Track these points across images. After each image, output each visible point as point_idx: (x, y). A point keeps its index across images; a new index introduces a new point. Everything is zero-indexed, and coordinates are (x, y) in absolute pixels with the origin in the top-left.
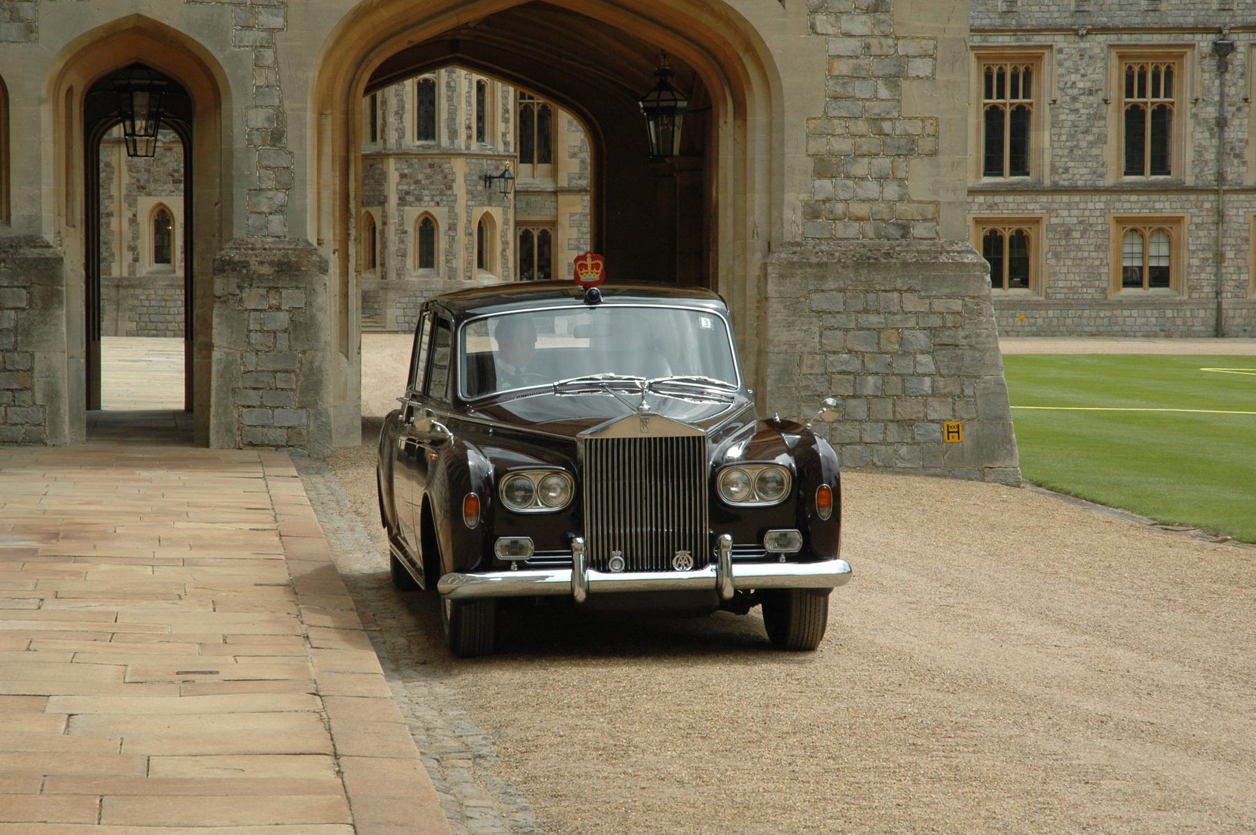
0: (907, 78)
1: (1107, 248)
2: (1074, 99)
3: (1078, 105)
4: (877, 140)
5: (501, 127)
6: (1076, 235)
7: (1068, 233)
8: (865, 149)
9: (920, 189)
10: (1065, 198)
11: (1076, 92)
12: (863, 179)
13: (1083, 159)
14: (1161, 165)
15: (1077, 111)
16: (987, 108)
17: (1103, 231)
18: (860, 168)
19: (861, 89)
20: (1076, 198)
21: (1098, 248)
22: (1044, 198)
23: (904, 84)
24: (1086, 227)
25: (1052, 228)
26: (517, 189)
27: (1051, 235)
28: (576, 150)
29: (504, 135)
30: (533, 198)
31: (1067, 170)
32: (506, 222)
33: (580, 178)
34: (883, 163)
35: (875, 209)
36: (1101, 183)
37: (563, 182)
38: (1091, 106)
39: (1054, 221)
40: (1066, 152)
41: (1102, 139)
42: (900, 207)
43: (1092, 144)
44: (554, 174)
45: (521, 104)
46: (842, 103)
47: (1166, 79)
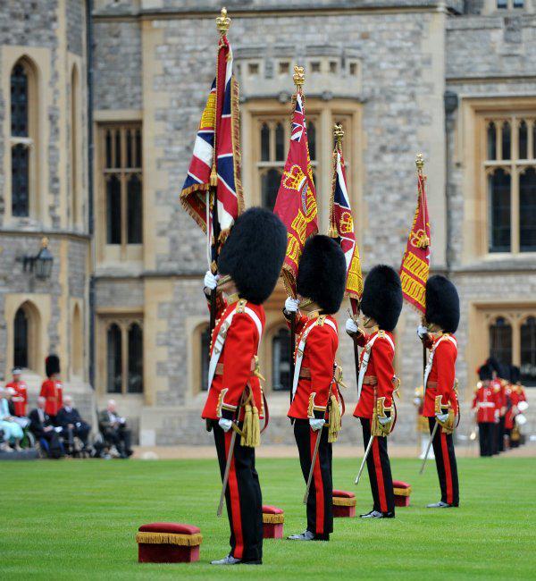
5: (47, 199)
16: (491, 171)
26: (98, 274)
28: (165, 227)
29: (52, 208)
30: (118, 286)
32: (56, 312)
33: (170, 260)
37: (151, 266)
44: (141, 256)
45: (106, 174)
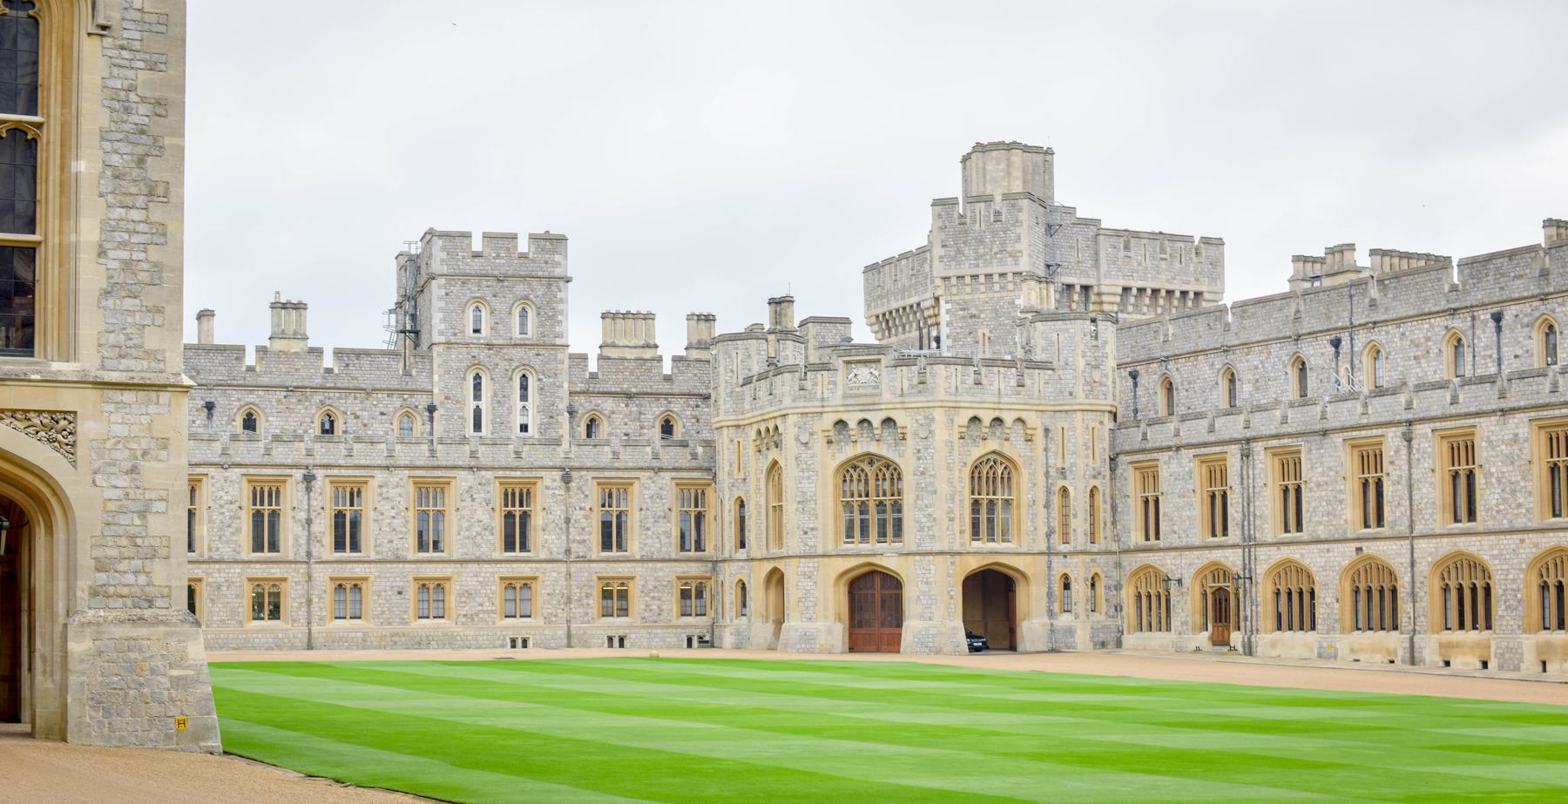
0: (151, 513)
1: (243, 596)
2: (221, 506)
3: (223, 510)
4: (133, 549)
6: (224, 588)
7: (219, 587)
8: (126, 555)
9: (159, 578)
10: (217, 566)
11: (222, 502)
12: (124, 572)
13: (227, 542)
14: (274, 547)
15: (223, 513)
17: (240, 587)
18: (123, 566)
19: (123, 519)
20: (224, 566)
21: (237, 596)
22: (204, 566)
23: (150, 516)
24: (230, 583)
25: (209, 585)
27: (209, 588)
31: (218, 549)
34: (137, 563)
35: (133, 590)
36: (238, 557)
38: (232, 511)
39: (210, 580)
40: (217, 538)
41: (239, 530)
42: (147, 589)
43: (233, 534)
46: (112, 527)
47: (274, 495)
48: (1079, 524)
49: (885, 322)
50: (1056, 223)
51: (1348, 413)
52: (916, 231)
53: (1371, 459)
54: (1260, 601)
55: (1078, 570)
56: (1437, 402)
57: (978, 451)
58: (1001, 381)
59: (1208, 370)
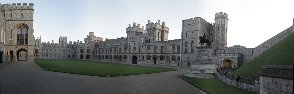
48: (93, 53)
49: (85, 42)
50: (94, 36)
51: (106, 47)
52: (86, 37)
53: (107, 50)
54: (101, 57)
55: (93, 55)
56: (110, 47)
57: (87, 49)
58: (89, 45)
59: (100, 45)
